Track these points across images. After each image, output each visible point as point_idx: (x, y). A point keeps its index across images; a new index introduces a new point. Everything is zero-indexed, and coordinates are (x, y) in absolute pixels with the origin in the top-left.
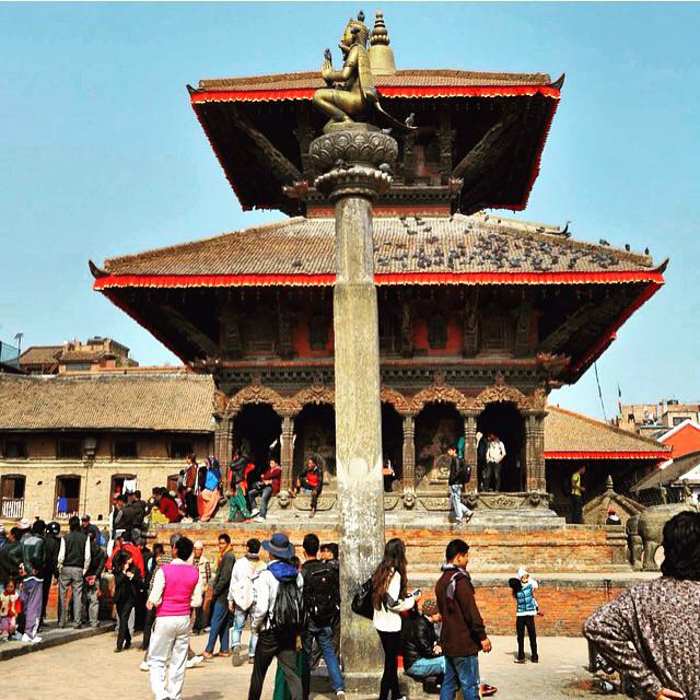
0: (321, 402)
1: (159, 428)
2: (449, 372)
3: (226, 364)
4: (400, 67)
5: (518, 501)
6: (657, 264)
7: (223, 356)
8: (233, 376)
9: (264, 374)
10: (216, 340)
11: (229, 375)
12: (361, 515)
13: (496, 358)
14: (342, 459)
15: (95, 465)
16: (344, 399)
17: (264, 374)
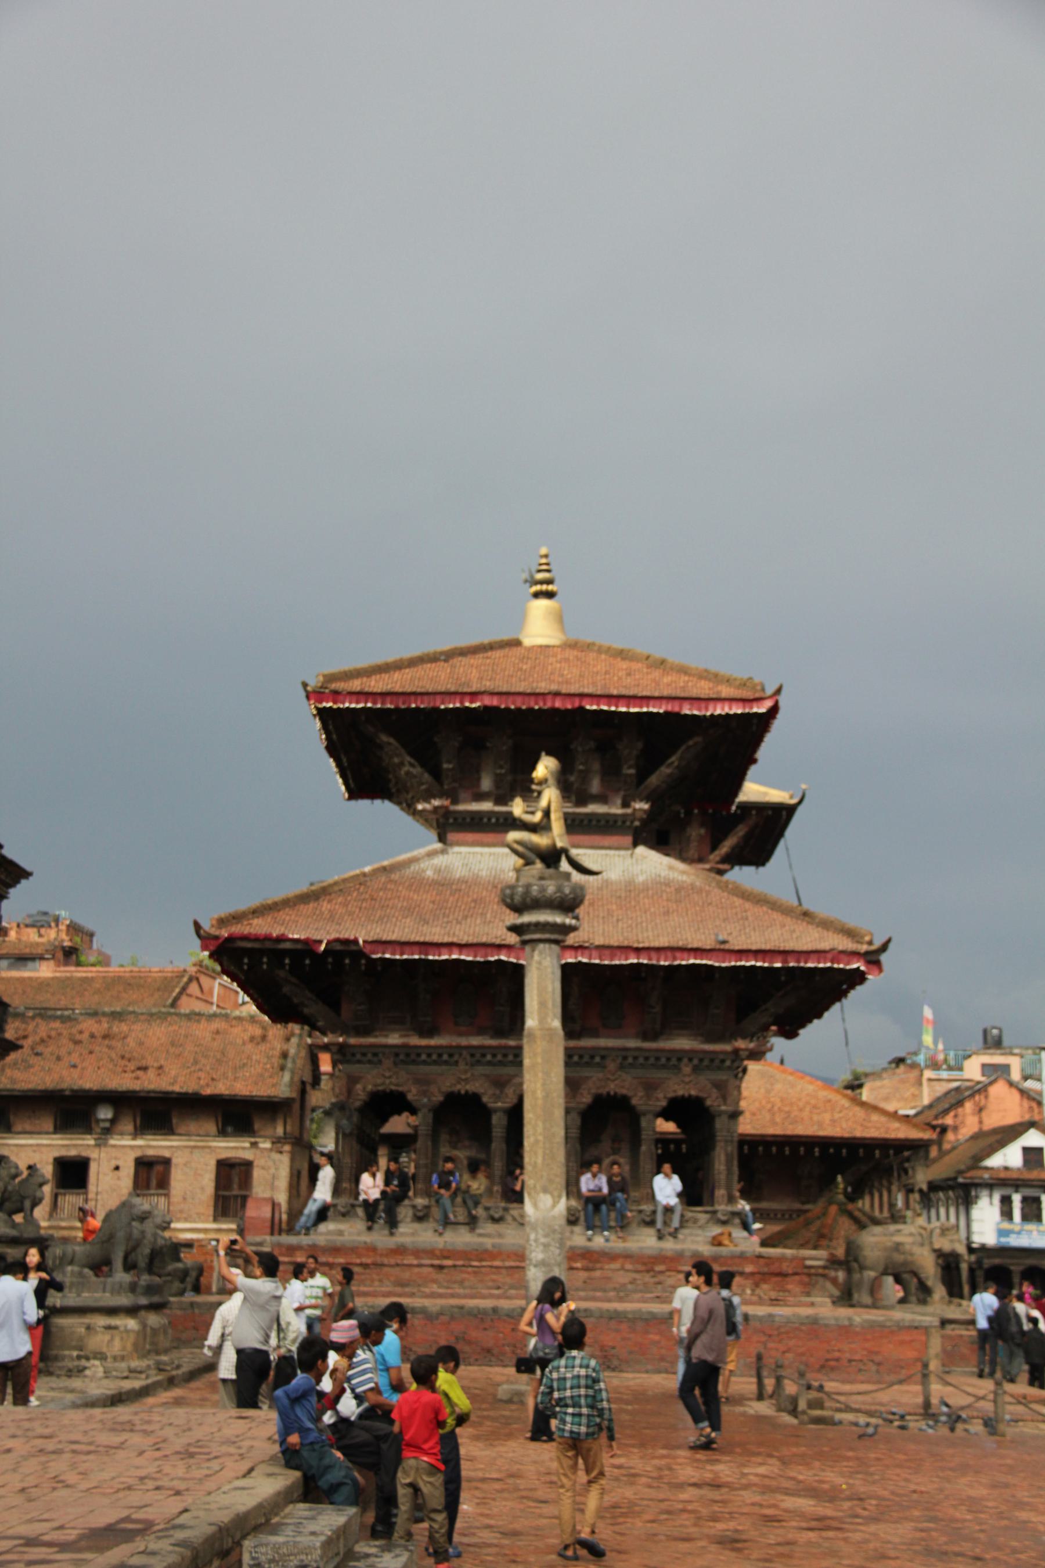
0: (467, 1092)
1: (208, 1091)
2: (625, 1058)
3: (352, 1041)
4: (573, 636)
5: (703, 1217)
6: (877, 944)
7: (345, 1031)
8: (358, 1056)
9: (397, 1055)
10: (335, 1006)
11: (353, 1055)
12: (546, 1246)
13: (683, 1043)
14: (529, 1194)
15: (112, 1142)
16: (532, 1139)
17: (397, 1055)
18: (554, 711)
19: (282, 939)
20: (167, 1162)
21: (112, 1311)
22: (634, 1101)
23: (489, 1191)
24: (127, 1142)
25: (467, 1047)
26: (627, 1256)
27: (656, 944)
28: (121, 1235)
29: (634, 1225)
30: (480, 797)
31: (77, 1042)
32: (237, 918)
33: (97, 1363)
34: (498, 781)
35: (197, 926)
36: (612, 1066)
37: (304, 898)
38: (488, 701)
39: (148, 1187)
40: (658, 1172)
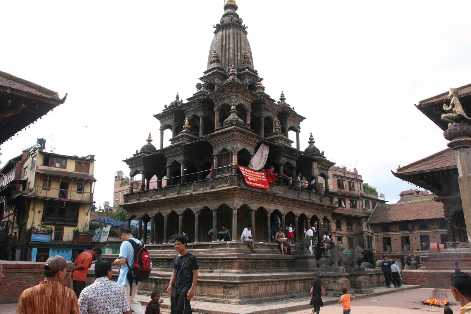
20: (428, 236)
24: (417, 232)
33: (331, 292)
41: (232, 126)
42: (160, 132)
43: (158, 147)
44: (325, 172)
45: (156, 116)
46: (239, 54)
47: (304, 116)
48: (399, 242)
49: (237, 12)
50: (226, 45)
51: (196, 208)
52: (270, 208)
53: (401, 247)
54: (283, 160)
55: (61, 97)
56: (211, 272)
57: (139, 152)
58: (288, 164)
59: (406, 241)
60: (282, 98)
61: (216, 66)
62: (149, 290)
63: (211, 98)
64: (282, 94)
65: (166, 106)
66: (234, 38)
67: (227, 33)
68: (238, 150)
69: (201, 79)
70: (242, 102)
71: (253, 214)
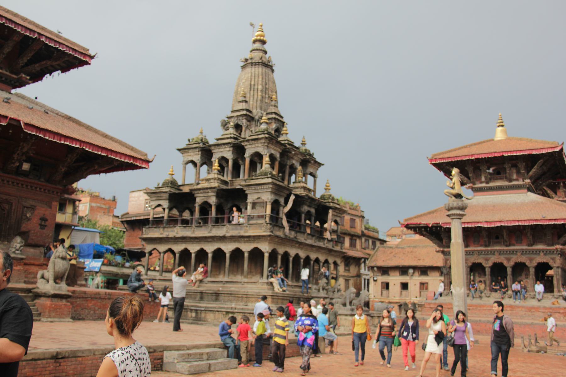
13: (540, 247)
18: (495, 157)
19: (420, 224)
20: (427, 283)
21: (346, 315)
22: (527, 264)
23: (485, 289)
25: (477, 250)
26: (523, 307)
27: (524, 219)
28: (348, 297)
29: (528, 298)
30: (481, 182)
31: (404, 254)
32: (410, 219)
34: (486, 178)
35: (399, 222)
36: (519, 254)
37: (430, 213)
38: (476, 157)
39: (423, 289)
40: (536, 283)
41: (268, 178)
42: (181, 167)
43: (180, 183)
44: (338, 219)
45: (179, 150)
46: (267, 96)
47: (322, 163)
48: (398, 287)
49: (266, 47)
50: (254, 85)
51: (228, 248)
52: (293, 252)
53: (399, 292)
54: (305, 208)
55: (150, 158)
56: (247, 305)
57: (160, 186)
58: (309, 212)
59: (405, 286)
60: (304, 144)
61: (244, 108)
62: (189, 320)
63: (243, 144)
64: (304, 138)
65: (189, 141)
66: (263, 79)
67: (257, 73)
68: (272, 201)
69: (229, 118)
70: (273, 152)
71: (280, 257)
